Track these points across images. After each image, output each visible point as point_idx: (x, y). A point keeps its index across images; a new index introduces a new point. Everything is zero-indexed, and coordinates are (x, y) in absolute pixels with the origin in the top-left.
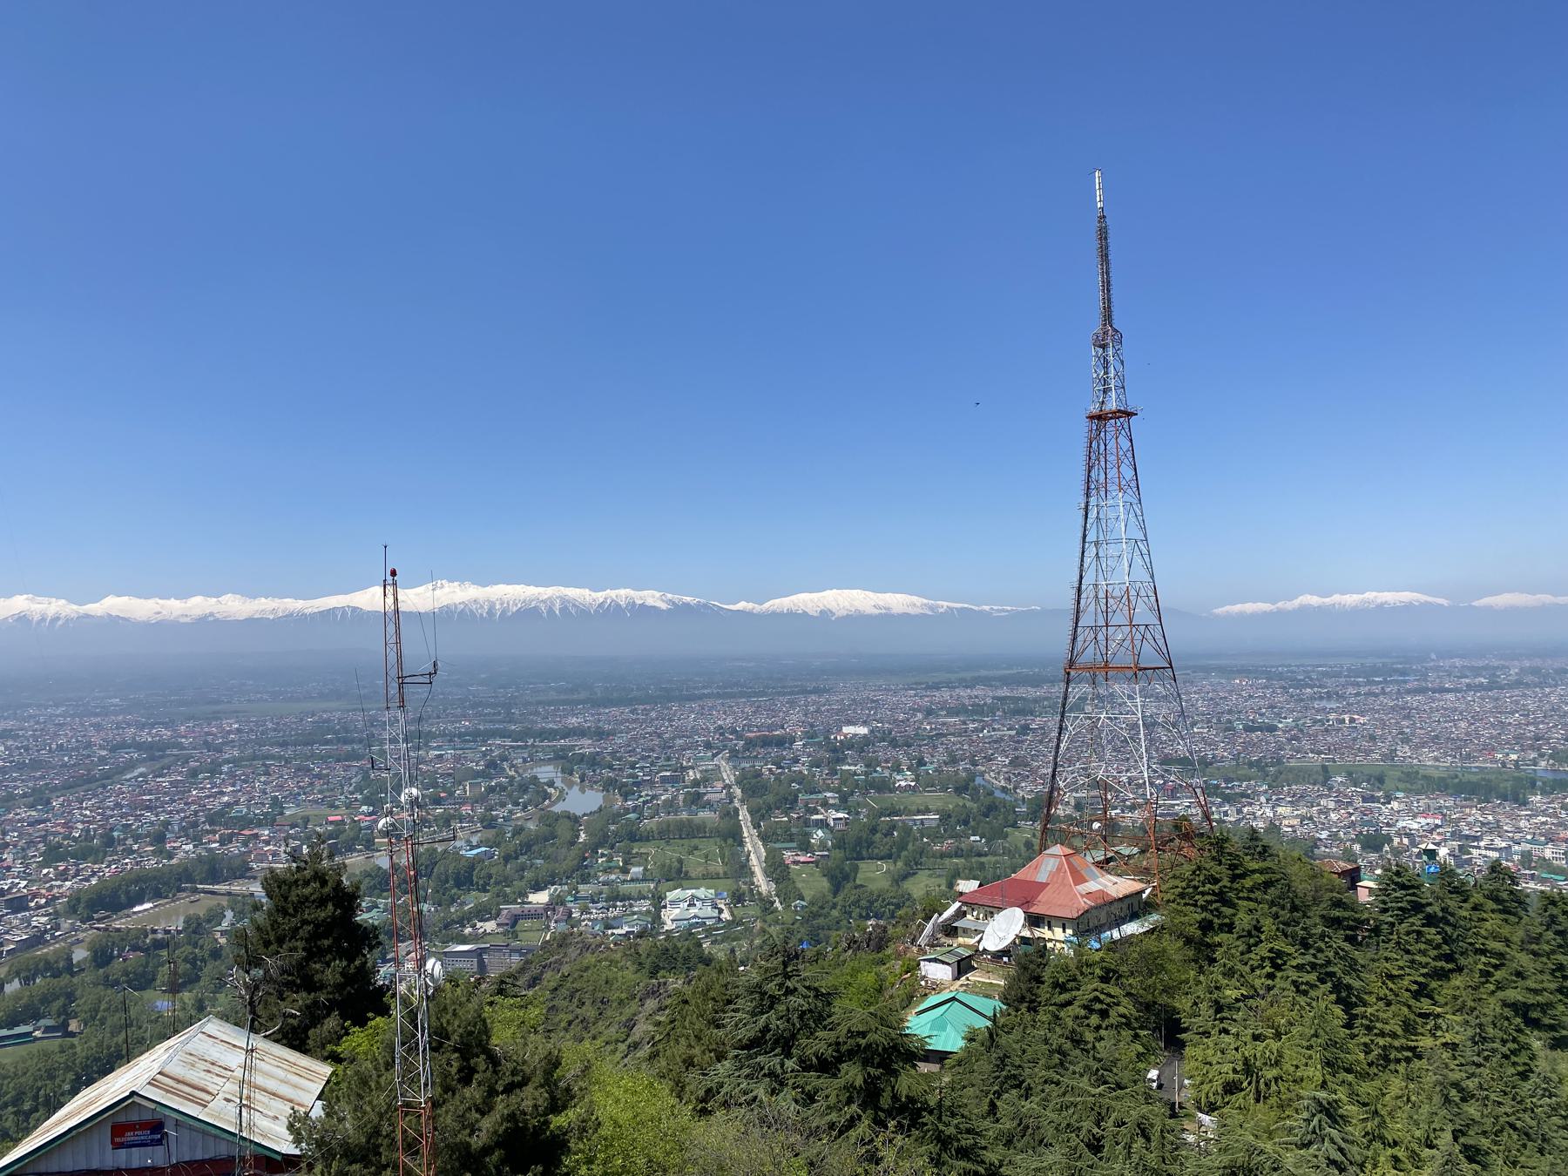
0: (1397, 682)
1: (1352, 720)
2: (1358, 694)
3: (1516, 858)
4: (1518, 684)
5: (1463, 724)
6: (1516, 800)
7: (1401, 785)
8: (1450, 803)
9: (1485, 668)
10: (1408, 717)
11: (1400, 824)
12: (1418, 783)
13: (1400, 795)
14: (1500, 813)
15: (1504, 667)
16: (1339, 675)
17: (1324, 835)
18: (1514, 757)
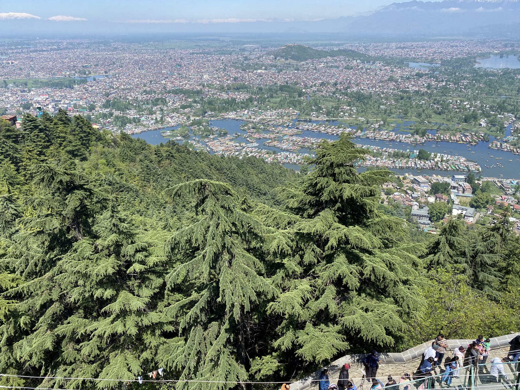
0: (26, 48)
1: (12, 63)
2: (13, 53)
3: (72, 106)
4: (66, 48)
5: (51, 63)
6: (70, 87)
7: (33, 86)
8: (50, 90)
9: (55, 43)
10: (32, 61)
11: (35, 99)
12: (40, 84)
13: (33, 89)
14: (66, 92)
15: (61, 42)
16: (4, 45)
17: (9, 106)
18: (68, 73)
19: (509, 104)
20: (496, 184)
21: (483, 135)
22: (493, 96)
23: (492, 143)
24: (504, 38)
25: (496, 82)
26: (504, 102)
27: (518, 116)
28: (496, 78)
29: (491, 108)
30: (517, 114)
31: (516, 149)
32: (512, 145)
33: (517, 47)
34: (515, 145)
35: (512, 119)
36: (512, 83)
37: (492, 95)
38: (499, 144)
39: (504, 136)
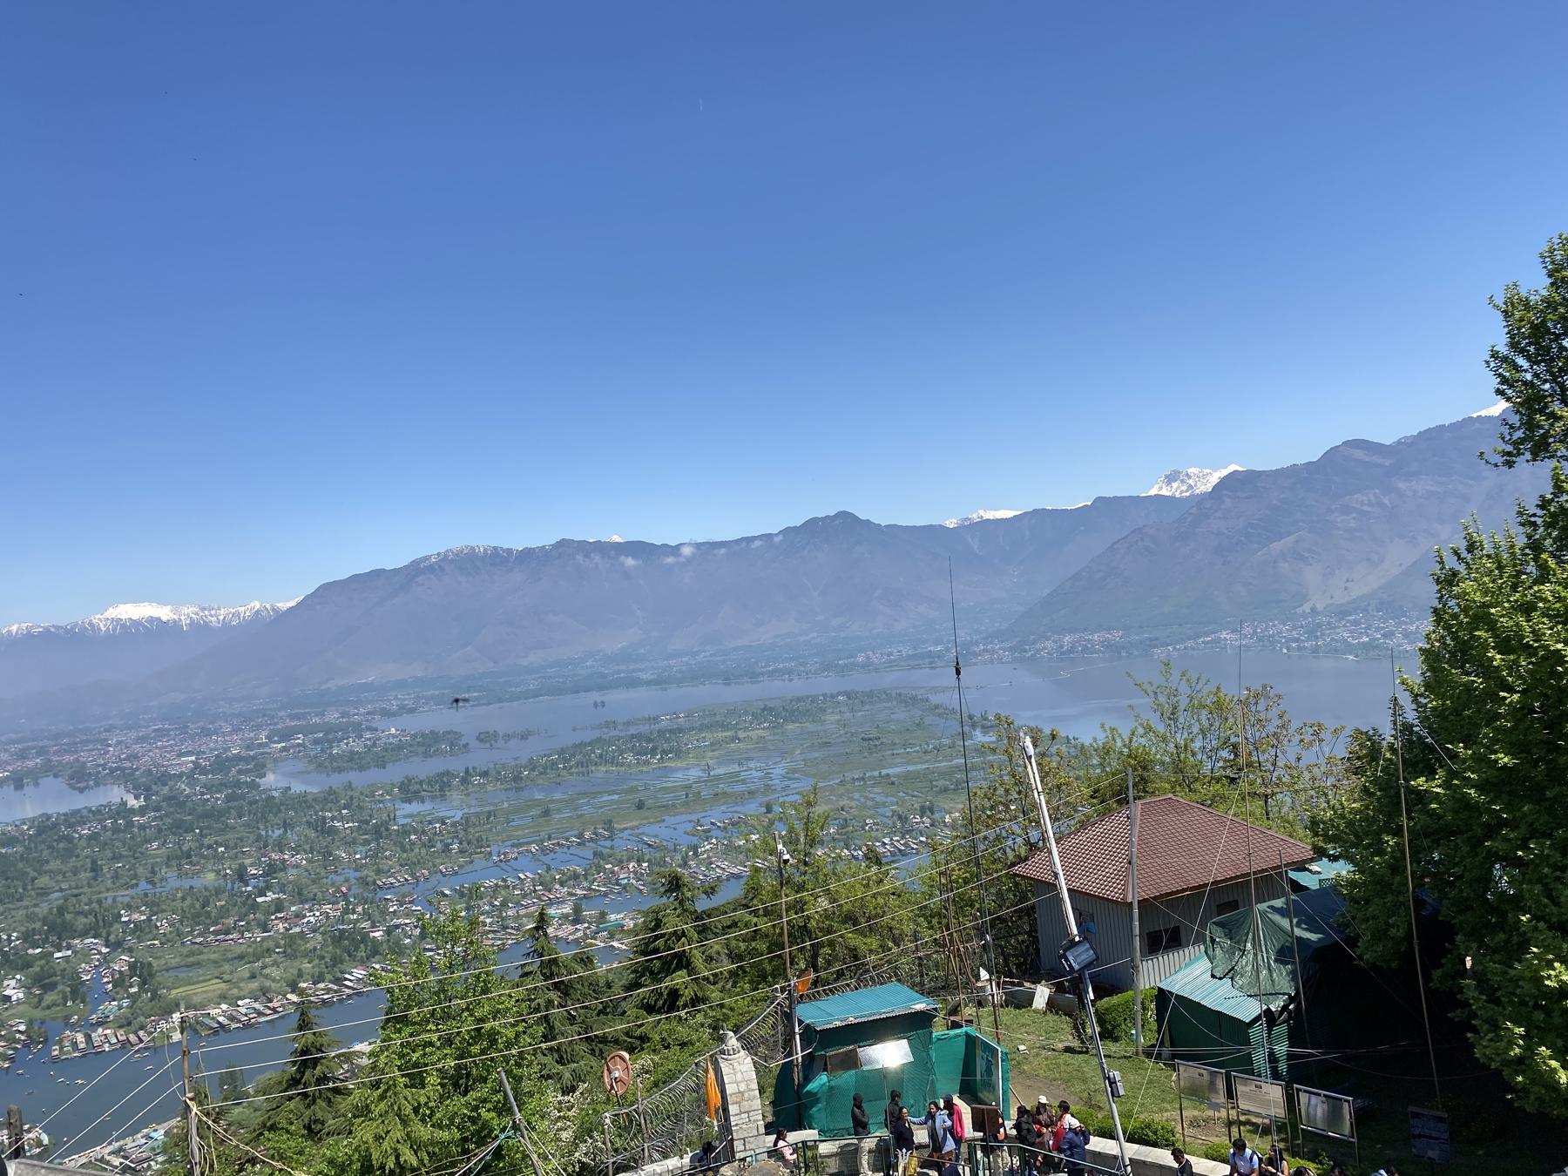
19: (79, 913)
20: (108, 1163)
21: (22, 1028)
22: (25, 903)
23: (61, 1041)
24: (13, 736)
25: (22, 858)
26: (61, 910)
27: (112, 938)
28: (19, 849)
29: (27, 938)
30: (109, 934)
31: (135, 1033)
32: (121, 1027)
33: (55, 753)
34: (129, 1024)
35: (100, 953)
36: (69, 854)
37: (20, 899)
38: (80, 1038)
39: (89, 1007)
